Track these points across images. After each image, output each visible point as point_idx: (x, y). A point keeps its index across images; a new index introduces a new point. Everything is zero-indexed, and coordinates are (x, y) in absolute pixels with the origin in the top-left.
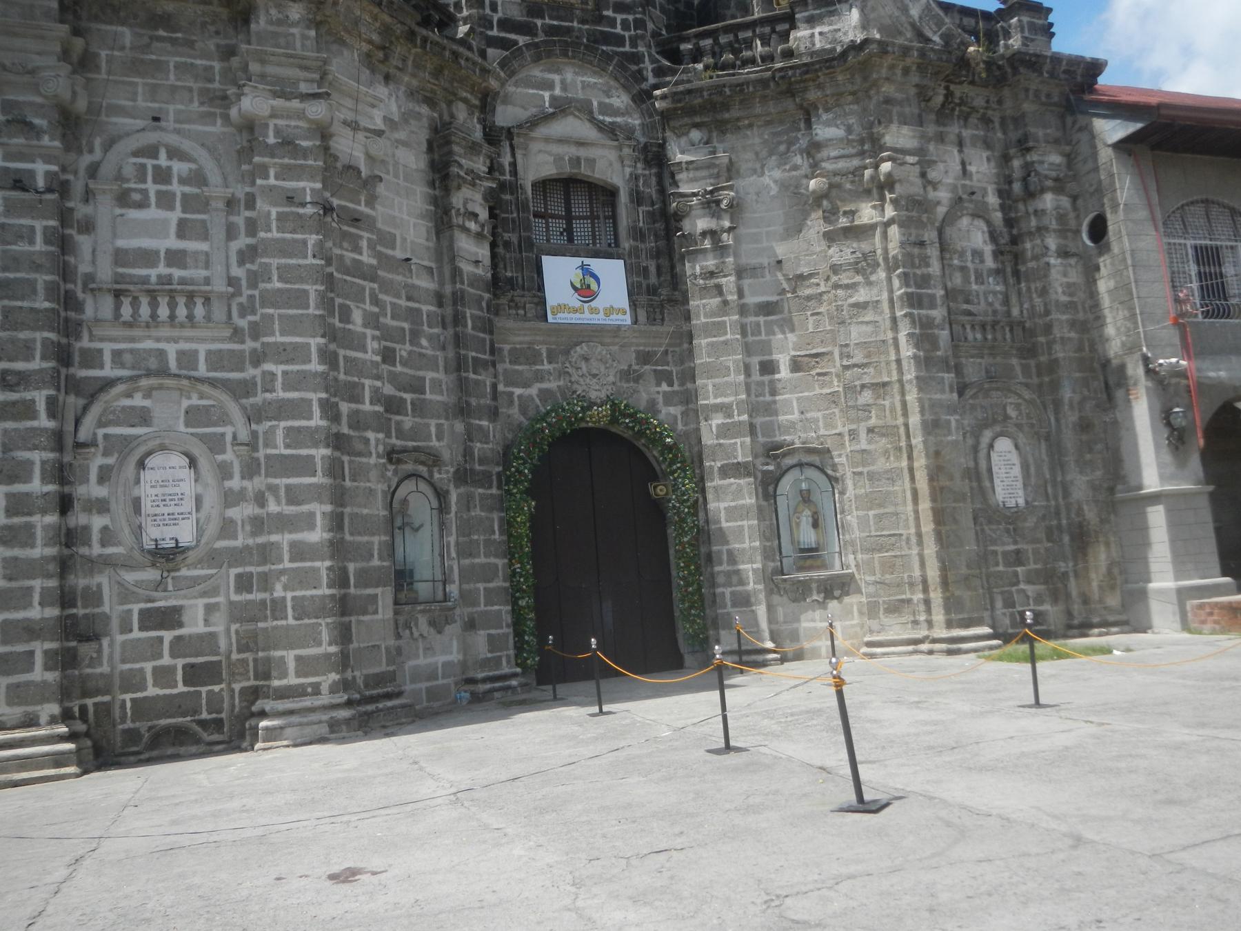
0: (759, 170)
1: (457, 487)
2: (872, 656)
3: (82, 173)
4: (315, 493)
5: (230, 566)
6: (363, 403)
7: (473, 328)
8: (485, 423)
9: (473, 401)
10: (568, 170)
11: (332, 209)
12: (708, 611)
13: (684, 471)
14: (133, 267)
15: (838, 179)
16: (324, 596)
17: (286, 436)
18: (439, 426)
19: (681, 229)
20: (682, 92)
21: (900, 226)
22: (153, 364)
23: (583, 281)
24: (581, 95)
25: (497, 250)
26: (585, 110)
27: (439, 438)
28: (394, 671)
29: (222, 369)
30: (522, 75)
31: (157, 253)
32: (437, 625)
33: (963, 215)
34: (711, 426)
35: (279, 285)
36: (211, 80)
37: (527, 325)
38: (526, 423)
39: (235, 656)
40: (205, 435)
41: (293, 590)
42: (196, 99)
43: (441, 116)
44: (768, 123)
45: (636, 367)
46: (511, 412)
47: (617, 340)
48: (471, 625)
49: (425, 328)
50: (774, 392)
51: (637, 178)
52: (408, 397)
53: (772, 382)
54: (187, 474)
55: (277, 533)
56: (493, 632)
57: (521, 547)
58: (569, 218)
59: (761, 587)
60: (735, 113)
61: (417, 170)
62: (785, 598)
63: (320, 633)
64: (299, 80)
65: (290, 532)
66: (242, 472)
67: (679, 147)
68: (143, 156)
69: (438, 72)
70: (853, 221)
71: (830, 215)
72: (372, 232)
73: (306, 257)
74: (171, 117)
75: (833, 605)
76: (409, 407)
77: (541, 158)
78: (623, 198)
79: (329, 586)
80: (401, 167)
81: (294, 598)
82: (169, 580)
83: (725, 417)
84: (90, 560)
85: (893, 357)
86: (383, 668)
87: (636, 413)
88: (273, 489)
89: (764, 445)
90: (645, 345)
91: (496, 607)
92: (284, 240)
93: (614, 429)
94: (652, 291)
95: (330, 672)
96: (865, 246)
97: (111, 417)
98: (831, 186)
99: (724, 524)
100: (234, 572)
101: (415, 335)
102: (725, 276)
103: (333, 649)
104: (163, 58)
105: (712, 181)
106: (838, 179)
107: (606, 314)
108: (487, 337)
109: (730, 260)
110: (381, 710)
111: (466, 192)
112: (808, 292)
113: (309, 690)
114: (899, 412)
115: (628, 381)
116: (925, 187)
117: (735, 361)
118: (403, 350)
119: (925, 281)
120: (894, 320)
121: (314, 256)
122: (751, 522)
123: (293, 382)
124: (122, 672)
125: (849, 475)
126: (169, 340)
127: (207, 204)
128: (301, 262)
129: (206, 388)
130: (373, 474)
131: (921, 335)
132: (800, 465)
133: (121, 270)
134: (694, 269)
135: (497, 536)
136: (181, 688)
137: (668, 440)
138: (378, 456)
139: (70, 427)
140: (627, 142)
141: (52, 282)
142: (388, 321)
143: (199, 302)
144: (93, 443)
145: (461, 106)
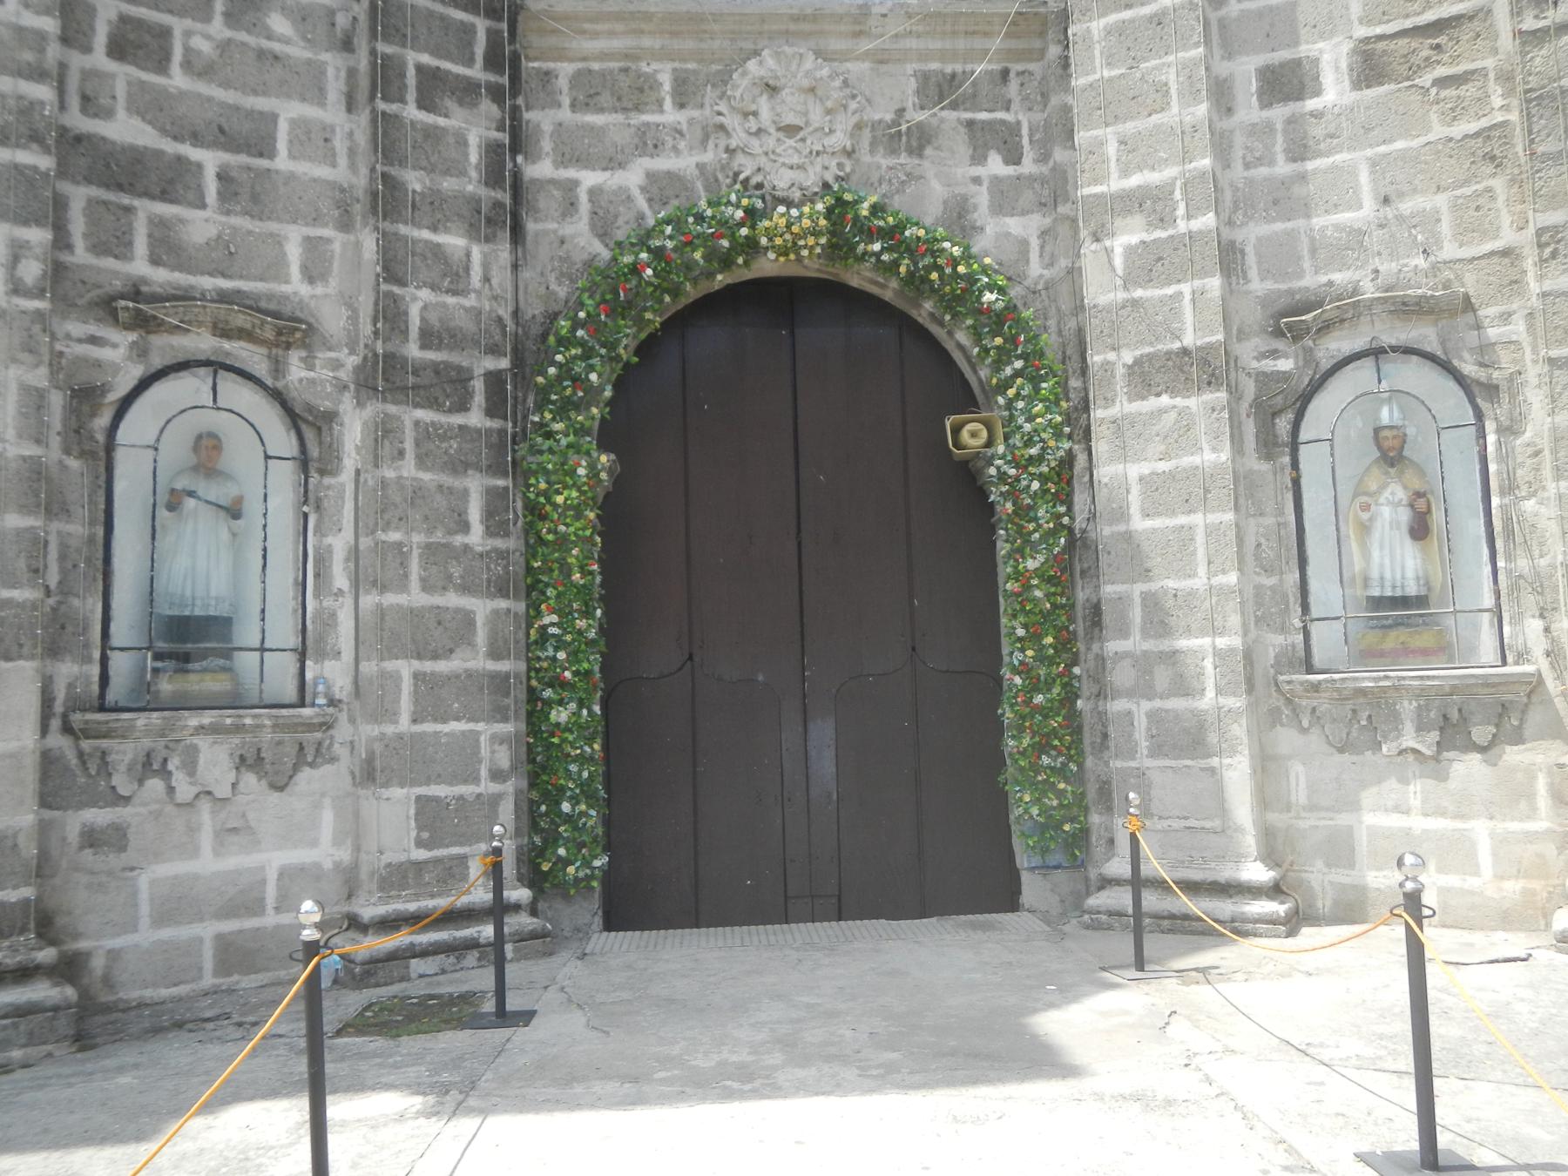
1: (360, 404)
8: (453, 241)
9: (414, 180)
12: (1089, 762)
13: (1035, 381)
18: (311, 244)
27: (310, 277)
28: (26, 902)
34: (1109, 252)
38: (606, 254)
46: (567, 230)
48: (369, 774)
50: (1299, 151)
52: (210, 160)
57: (569, 575)
59: (1236, 702)
62: (1315, 740)
75: (1467, 768)
76: (211, 187)
83: (1151, 226)
87: (900, 227)
89: (1265, 301)
90: (943, 56)
99: (1139, 524)
108: (481, 25)
115: (894, 152)
117: (1183, 66)
122: (1214, 518)
125: (1533, 372)
132: (1376, 353)
135: (476, 537)
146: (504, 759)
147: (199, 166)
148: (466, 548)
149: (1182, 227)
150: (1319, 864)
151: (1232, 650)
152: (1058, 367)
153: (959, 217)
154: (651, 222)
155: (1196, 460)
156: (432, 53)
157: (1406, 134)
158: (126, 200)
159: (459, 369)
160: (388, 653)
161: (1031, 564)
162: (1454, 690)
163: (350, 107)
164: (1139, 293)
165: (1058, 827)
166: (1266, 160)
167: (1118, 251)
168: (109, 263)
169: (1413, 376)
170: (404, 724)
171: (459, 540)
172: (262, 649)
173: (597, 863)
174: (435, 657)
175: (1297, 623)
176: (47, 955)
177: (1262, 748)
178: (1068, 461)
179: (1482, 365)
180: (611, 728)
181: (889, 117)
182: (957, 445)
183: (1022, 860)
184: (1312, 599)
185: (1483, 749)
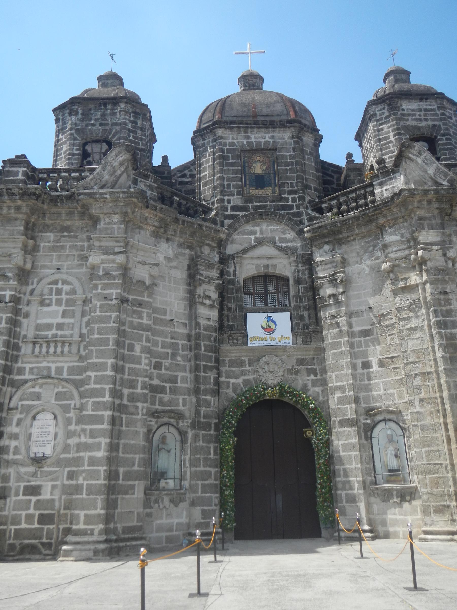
0: (359, 262)
1: (192, 430)
2: (426, 540)
3: (28, 293)
4: (102, 433)
5: (65, 467)
6: (137, 389)
7: (205, 351)
8: (208, 398)
9: (202, 387)
10: (262, 271)
11: (127, 301)
12: (335, 504)
13: (321, 423)
14: (42, 331)
15: (397, 262)
16: (101, 485)
17: (92, 406)
18: (184, 400)
19: (319, 295)
20: (317, 228)
21: (431, 284)
22: (45, 373)
23: (267, 324)
24: (270, 235)
25: (224, 312)
26: (273, 242)
27: (184, 405)
29: (74, 374)
30: (241, 229)
31: (52, 325)
32: (175, 502)
34: (334, 398)
35: (97, 336)
36: (82, 251)
37: (237, 347)
38: (235, 397)
39: (62, 511)
40: (63, 405)
41: (87, 480)
42: (76, 259)
43: (196, 253)
44: (363, 237)
45: (296, 367)
46: (228, 391)
47: (285, 353)
48: (193, 504)
49: (180, 352)
50: (369, 379)
51: (298, 271)
52: (168, 385)
53: (368, 373)
54: (53, 422)
55: (83, 452)
56: (205, 508)
57: (228, 463)
58: (266, 294)
59: (361, 491)
60: (345, 235)
61: (181, 279)
62: (378, 500)
63: (97, 503)
64: (115, 247)
65: (89, 452)
66: (76, 422)
67: (319, 254)
69: (193, 234)
70: (407, 283)
71: (395, 281)
72: (149, 309)
73: (110, 323)
74: (65, 267)
75: (406, 505)
78: (291, 282)
79: (104, 479)
80: (172, 278)
81: (87, 485)
82: (39, 472)
84: (7, 461)
85: (432, 358)
86: (135, 523)
87: (293, 392)
88: (84, 431)
89: (365, 408)
91: (208, 495)
92: (101, 316)
93: (281, 399)
94: (306, 327)
95: (100, 524)
96: (414, 296)
97: (25, 397)
98: (394, 266)
99: (342, 454)
100: (67, 469)
101: (174, 355)
102: (341, 317)
103: (102, 512)
105: (334, 269)
106: (397, 262)
107: (279, 340)
108: (213, 355)
109: (343, 308)
110: (129, 546)
111: (205, 286)
112: (387, 323)
113: (89, 532)
114: (437, 390)
115: (291, 374)
116: (446, 261)
117: (346, 362)
118: (166, 363)
120: (432, 336)
121: (114, 322)
122: (356, 453)
123: (98, 380)
124: (12, 515)
126: (53, 362)
127: (75, 302)
129: (64, 383)
130: (139, 424)
131: (447, 344)
133: (37, 333)
134: (325, 314)
135: (212, 456)
136: (36, 525)
137: (311, 406)
138: (143, 415)
139: (7, 401)
140: (293, 255)
141: (6, 340)
142: (160, 349)
143: (67, 345)
144: (16, 409)
145: (206, 247)
146: (217, 501)
147: (166, 387)
148: (210, 458)
149: (347, 394)
150: (380, 526)
151: (360, 481)
152: (326, 420)
153: (305, 389)
154: (244, 390)
155: (352, 441)
156: (206, 362)
157: (388, 377)
158: (155, 395)
159: (210, 423)
160: (197, 480)
161: (321, 461)
162: (402, 489)
163: (190, 372)
164: (340, 406)
165: (329, 519)
166: (363, 380)
167: (336, 398)
168: (153, 407)
169: (392, 425)
170: (199, 494)
171: (209, 457)
172: (174, 479)
173: (234, 525)
174: (205, 480)
175: (373, 475)
176: (144, 535)
177: (368, 501)
178: (328, 439)
179: (404, 424)
180: (236, 496)
181: (291, 367)
182: (306, 435)
183: (322, 526)
184: (376, 470)
185: (409, 502)
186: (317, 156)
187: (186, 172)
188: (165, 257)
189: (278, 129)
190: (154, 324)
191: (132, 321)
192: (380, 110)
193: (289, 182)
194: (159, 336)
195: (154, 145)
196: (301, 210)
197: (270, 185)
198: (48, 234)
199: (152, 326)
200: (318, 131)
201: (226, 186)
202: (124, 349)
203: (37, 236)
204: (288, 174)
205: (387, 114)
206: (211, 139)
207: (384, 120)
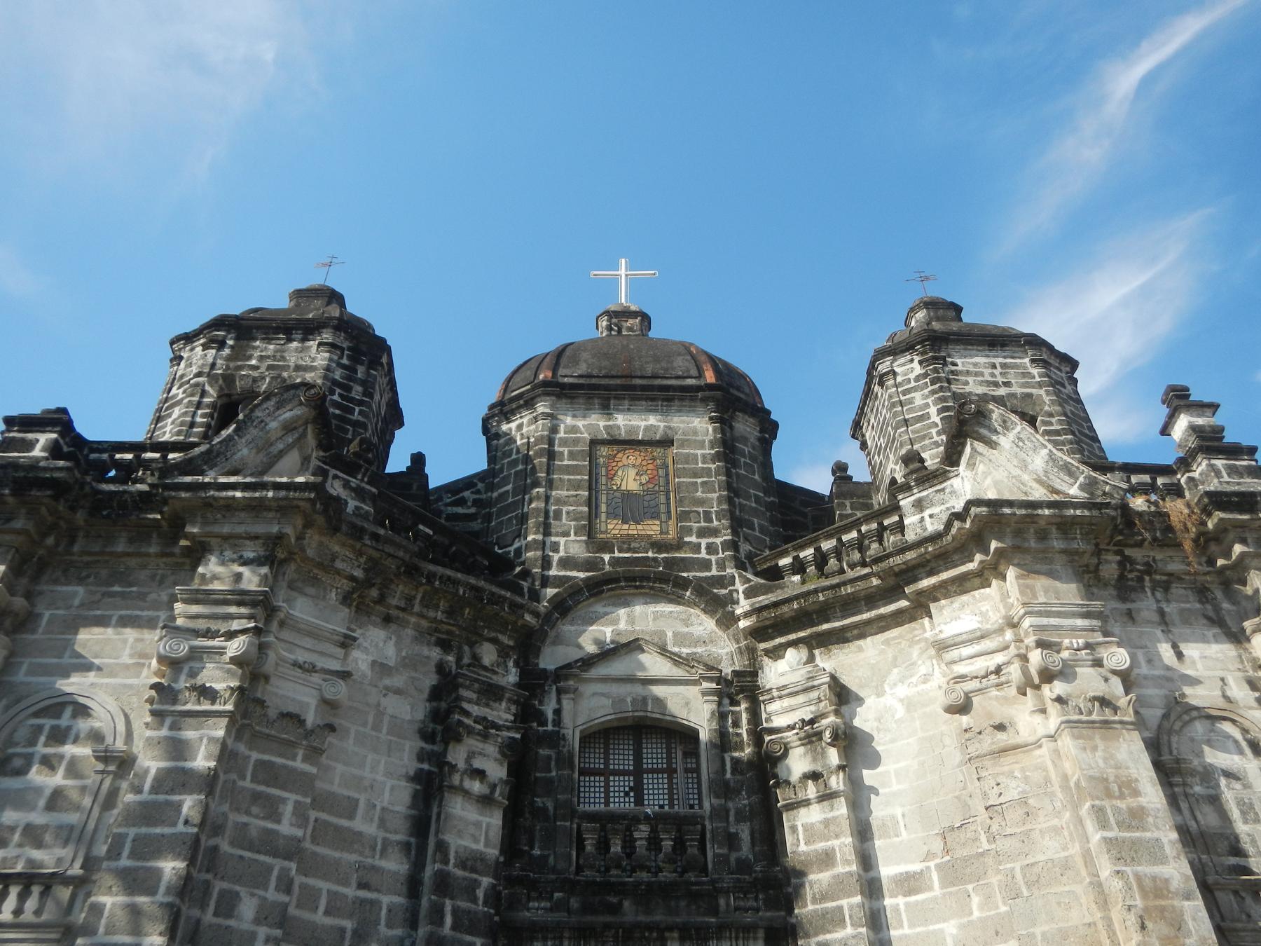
7: (454, 928)
24: (652, 626)
33: (1192, 720)
61: (410, 722)
68: (44, 717)
77: (596, 702)
80: (386, 719)
104: (107, 613)
105: (813, 708)
111: (472, 743)
116: (1106, 680)
119: (1136, 817)
128: (167, 830)
142: (320, 918)
186: (767, 466)
187: (467, 494)
188: (374, 663)
189: (677, 402)
190: (314, 840)
191: (246, 825)
192: (902, 365)
193: (701, 510)
194: (325, 877)
195: (398, 433)
196: (728, 571)
197: (655, 516)
198: (70, 588)
199: (307, 844)
200: (769, 413)
201: (551, 514)
202: (203, 906)
203: (40, 593)
204: (699, 494)
205: (918, 370)
206: (525, 420)
207: (913, 384)
